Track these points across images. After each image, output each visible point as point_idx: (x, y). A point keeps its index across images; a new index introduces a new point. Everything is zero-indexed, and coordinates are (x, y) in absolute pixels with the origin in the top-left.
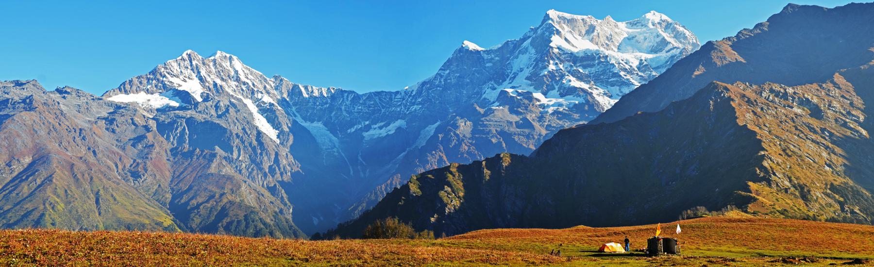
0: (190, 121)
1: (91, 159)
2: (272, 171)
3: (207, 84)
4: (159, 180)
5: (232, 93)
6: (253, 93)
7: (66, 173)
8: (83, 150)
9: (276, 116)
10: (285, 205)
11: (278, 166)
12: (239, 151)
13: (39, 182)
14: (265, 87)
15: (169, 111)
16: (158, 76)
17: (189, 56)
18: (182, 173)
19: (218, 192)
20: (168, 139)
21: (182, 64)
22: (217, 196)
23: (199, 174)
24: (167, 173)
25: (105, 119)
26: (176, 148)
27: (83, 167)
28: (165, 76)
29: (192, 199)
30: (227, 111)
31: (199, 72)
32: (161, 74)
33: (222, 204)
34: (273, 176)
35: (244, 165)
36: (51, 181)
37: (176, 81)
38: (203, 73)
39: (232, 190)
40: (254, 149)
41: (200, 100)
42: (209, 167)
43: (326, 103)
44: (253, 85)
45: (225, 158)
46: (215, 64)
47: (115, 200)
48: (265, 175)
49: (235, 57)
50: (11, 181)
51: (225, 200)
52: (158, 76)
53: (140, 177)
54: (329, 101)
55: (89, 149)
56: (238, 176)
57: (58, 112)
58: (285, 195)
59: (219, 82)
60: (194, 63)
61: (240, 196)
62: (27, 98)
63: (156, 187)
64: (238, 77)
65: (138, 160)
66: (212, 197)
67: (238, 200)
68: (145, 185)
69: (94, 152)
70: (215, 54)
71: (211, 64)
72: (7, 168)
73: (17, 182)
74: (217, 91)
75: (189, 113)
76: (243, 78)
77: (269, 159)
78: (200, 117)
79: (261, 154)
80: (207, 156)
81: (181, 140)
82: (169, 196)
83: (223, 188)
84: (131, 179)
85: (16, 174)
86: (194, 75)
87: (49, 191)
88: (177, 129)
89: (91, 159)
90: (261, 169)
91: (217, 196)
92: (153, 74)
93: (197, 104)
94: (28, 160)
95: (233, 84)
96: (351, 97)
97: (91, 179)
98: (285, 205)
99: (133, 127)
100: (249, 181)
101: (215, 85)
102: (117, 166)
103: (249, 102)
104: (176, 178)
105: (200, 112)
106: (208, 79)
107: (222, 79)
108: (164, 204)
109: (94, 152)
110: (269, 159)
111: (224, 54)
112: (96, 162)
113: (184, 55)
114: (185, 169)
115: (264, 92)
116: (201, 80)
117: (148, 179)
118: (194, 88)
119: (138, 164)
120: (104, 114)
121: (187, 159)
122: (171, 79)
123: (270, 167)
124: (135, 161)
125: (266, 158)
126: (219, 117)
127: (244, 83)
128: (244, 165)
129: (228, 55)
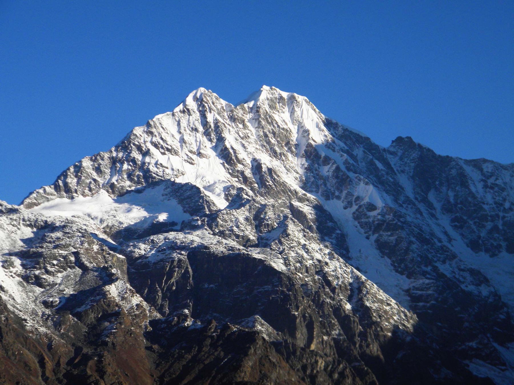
3: (240, 167)
12: (310, 327)
16: (136, 155)
17: (200, 101)
20: (150, 299)
21: (184, 123)
28: (146, 153)
31: (221, 139)
32: (139, 148)
35: (321, 364)
37: (176, 162)
38: (231, 140)
41: (220, 203)
45: (276, 345)
46: (257, 120)
49: (300, 98)
52: (136, 155)
59: (267, 161)
60: (210, 118)
65: (85, 350)
70: (255, 94)
74: (262, 182)
75: (196, 238)
79: (363, 335)
88: (170, 275)
99: (78, 271)
101: (257, 166)
102: (42, 363)
105: (222, 234)
106: (242, 155)
107: (274, 154)
113: (190, 101)
116: (227, 156)
119: (86, 358)
121: (189, 350)
122: (163, 159)
128: (321, 364)
129: (285, 95)
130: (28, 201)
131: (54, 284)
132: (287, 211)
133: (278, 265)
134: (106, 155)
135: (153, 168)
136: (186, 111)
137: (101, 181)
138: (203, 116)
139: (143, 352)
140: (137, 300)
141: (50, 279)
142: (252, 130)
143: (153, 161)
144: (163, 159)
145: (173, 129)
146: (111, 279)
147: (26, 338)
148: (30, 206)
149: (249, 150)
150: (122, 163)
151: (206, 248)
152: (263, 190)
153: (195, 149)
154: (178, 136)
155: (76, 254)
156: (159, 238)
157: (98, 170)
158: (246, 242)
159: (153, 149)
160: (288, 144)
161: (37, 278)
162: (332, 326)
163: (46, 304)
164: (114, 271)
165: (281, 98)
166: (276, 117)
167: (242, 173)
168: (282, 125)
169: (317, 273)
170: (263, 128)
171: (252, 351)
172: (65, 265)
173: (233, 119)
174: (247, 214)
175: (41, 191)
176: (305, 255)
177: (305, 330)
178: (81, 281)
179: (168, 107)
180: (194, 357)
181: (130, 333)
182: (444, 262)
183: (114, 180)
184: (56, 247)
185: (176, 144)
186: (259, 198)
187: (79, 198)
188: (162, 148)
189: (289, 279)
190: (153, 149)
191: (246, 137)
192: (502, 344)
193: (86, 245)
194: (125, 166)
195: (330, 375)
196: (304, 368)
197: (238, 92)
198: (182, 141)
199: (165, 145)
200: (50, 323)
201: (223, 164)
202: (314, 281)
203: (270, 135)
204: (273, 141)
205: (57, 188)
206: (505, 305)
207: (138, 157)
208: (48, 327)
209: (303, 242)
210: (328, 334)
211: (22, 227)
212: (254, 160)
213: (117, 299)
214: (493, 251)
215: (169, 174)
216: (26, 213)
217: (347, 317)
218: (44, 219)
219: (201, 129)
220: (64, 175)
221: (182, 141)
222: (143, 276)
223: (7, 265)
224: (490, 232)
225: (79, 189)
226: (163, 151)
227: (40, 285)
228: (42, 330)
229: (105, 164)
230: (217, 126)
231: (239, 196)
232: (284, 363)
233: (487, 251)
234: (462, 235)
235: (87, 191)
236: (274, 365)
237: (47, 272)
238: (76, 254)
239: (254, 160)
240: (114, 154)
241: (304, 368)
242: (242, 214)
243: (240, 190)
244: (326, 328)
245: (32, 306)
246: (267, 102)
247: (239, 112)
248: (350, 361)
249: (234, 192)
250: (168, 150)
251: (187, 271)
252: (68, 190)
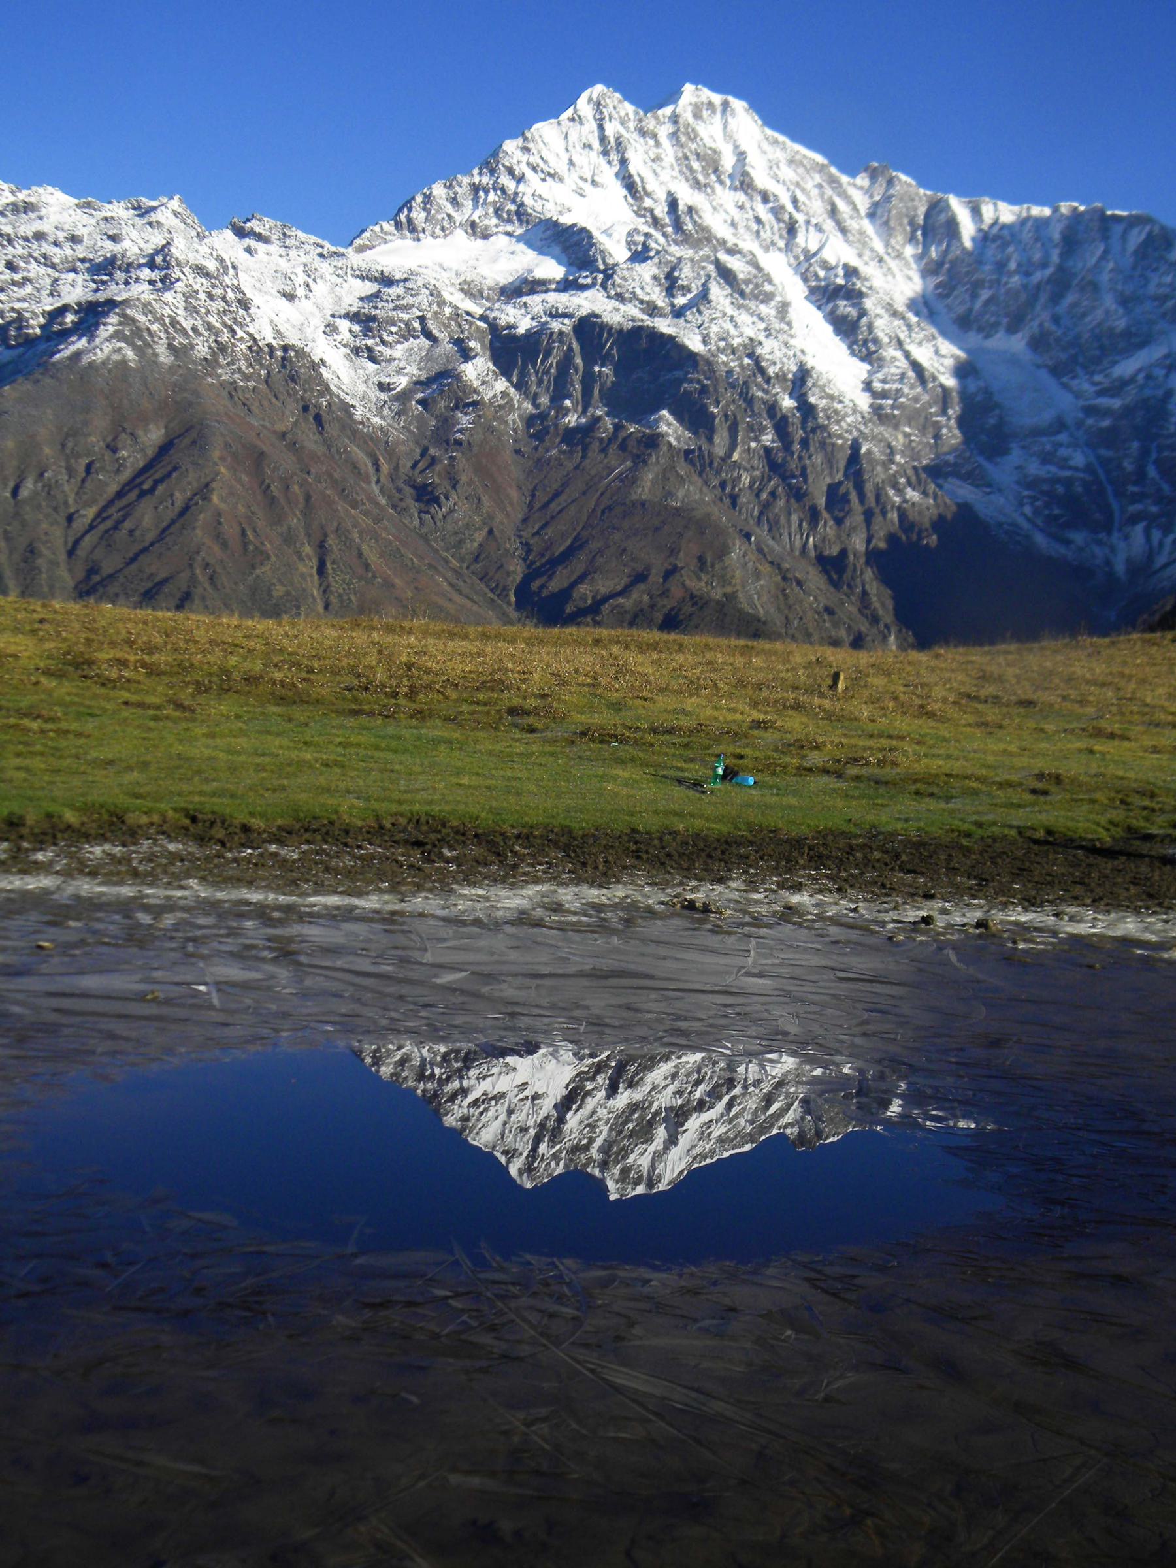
0: (588, 329)
1: (310, 439)
2: (835, 498)
3: (648, 202)
4: (491, 517)
5: (721, 230)
6: (792, 230)
7: (245, 478)
8: (291, 416)
9: (863, 313)
10: (875, 620)
11: (859, 487)
12: (733, 430)
13: (179, 498)
14: (833, 212)
15: (532, 292)
16: (505, 180)
17: (598, 105)
18: (557, 495)
19: (658, 565)
20: (520, 386)
21: (573, 137)
22: (656, 578)
23: (605, 502)
24: (514, 494)
25: (354, 317)
26: (543, 416)
27: (287, 462)
28: (520, 179)
29: (581, 578)
30: (704, 296)
31: (623, 162)
32: (510, 171)
33: (668, 604)
34: (839, 522)
35: (746, 479)
36: (206, 498)
39: (701, 559)
40: (781, 425)
41: (619, 253)
42: (634, 481)
43: (1044, 265)
44: (795, 201)
45: (688, 452)
46: (674, 135)
47: (367, 566)
48: (814, 516)
49: (739, 105)
50: (120, 494)
51: (677, 592)
52: (505, 180)
53: (436, 500)
54: (1055, 257)
55: (306, 409)
56: (722, 516)
57: (230, 295)
58: (873, 588)
59: (686, 196)
60: (611, 129)
61: (725, 581)
62: (157, 252)
63: (480, 536)
64: (745, 174)
65: (432, 452)
66: (640, 578)
67: (717, 594)
68: (449, 527)
69: (318, 418)
70: (673, 96)
71: (664, 131)
72: (108, 455)
73: (132, 496)
74: (678, 225)
76: (762, 179)
77: (830, 461)
78: (616, 314)
79: (805, 443)
80: (631, 444)
81: (559, 392)
82: (517, 569)
83: (673, 552)
84: (414, 507)
85: (126, 475)
86: (609, 175)
87: (199, 534)
88: (548, 354)
89: (310, 439)
90: (798, 495)
91: (656, 578)
92: (492, 172)
93: (609, 273)
94: (154, 435)
95: (728, 198)
96: (1136, 237)
97: (308, 498)
98: (875, 620)
99: (424, 342)
100: (761, 533)
101: (673, 204)
103: (779, 268)
104: (541, 507)
105: (620, 297)
107: (697, 185)
108: (502, 593)
109: (318, 418)
110: (830, 461)
111: (706, 94)
112: (321, 450)
113: (583, 105)
114: (565, 485)
115: (829, 225)
116: (630, 185)
117: (458, 508)
118: (607, 218)
119: (433, 461)
120: (351, 303)
123: (832, 490)
124: (424, 452)
125: (818, 459)
126: (678, 313)
127: (765, 198)
128: (746, 479)
129: (717, 98)
130: (358, 242)
131: (391, 360)
132: (711, 268)
133: (694, 344)
134: (466, 180)
135: (528, 201)
136: (576, 119)
137: (458, 217)
138: (601, 127)
139: (508, 455)
140: (501, 385)
141: (387, 352)
142: (669, 151)
143: (529, 191)
144: (544, 189)
145: (557, 143)
146: (466, 355)
147: (355, 432)
148: (361, 249)
149: (664, 180)
150: (487, 192)
151: (597, 316)
152: (679, 237)
153: (588, 176)
154: (565, 157)
155: (422, 319)
156: (535, 301)
157: (454, 201)
158: (652, 309)
159: (529, 174)
160: (716, 171)
161: (369, 349)
162: (762, 430)
163: (382, 387)
164: (472, 344)
165: (710, 105)
166: (702, 130)
167: (651, 211)
168: (709, 143)
169: (750, 356)
170: (682, 146)
171: (654, 459)
172: (407, 333)
173: (643, 133)
174: (655, 271)
175: (377, 228)
176: (733, 331)
177: (726, 434)
178: (428, 357)
179: (553, 112)
180: (576, 468)
181: (492, 430)
182: (920, 344)
183: (475, 217)
184: (396, 308)
185: (560, 166)
186: (673, 249)
187: (427, 240)
188: (542, 171)
189: (709, 363)
190: (529, 174)
191: (657, 159)
192: (989, 458)
193: (435, 307)
194: (492, 197)
195: (757, 496)
196: (723, 485)
197: (652, 94)
198: (571, 163)
199: (546, 168)
200: (386, 412)
201: (625, 197)
202: (741, 366)
203: (692, 158)
204: (696, 165)
205: (398, 225)
206: (997, 406)
207: (511, 185)
208: (383, 418)
209: (730, 311)
210: (756, 439)
211: (350, 278)
212: (670, 194)
213: (476, 383)
214: (988, 330)
215: (550, 211)
216: (354, 259)
217: (784, 418)
218: (380, 269)
219: (596, 144)
220: (408, 204)
221: (571, 163)
222: (510, 351)
223: (331, 330)
224: (988, 302)
225: (429, 228)
226: (543, 176)
227: (373, 359)
228: (377, 421)
229: (462, 190)
230: (619, 144)
231: (646, 248)
232: (695, 478)
233: (980, 329)
234: (949, 308)
235: (438, 231)
236: (682, 480)
237: (383, 342)
238: (422, 319)
239: (670, 194)
240: (476, 179)
241: (723, 485)
242: (647, 271)
243: (647, 235)
244: (756, 431)
245: (362, 388)
246: (690, 109)
247: (650, 123)
248: (784, 478)
249: (641, 239)
250: (550, 175)
251: (570, 349)
252: (412, 227)
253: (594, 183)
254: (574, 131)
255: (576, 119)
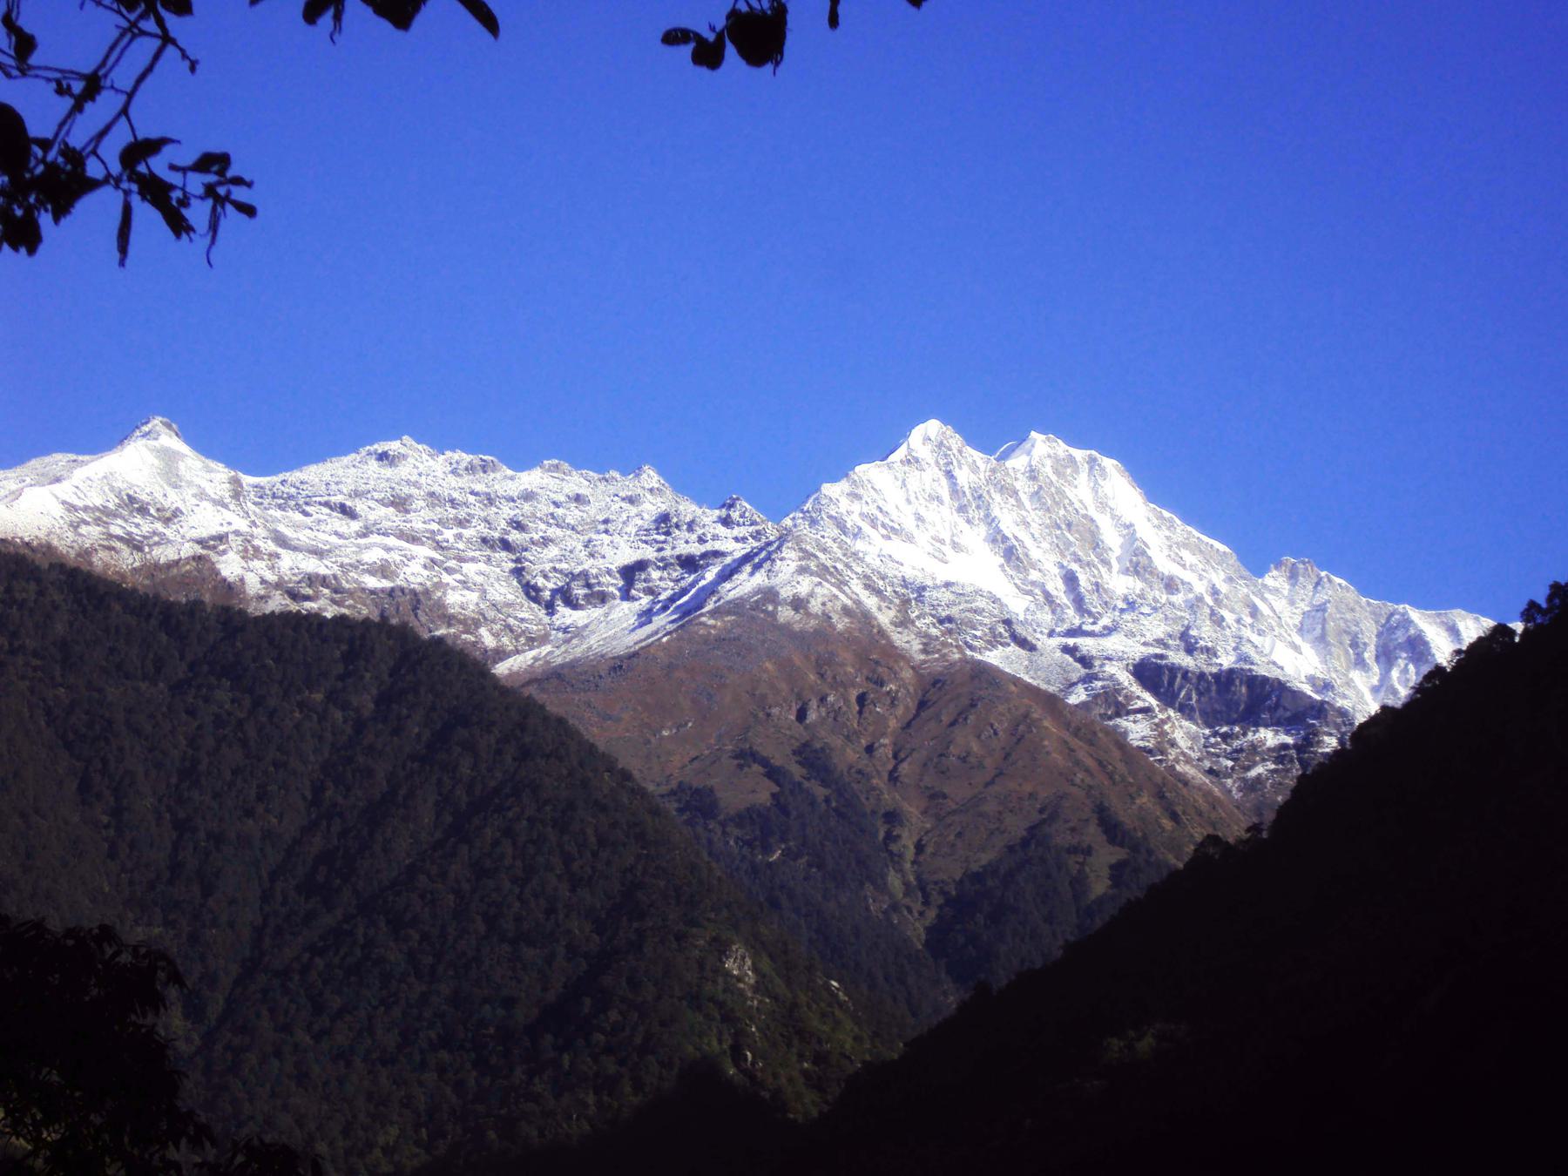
3: (1034, 575)
31: (990, 520)
49: (1109, 463)
71: (1023, 486)
86: (975, 537)
129: (1079, 454)
136: (911, 461)
159: (866, 528)
165: (1071, 459)
170: (1048, 510)
188: (884, 525)
199: (887, 521)
226: (884, 532)
246: (1048, 462)
253: (956, 546)
254: (914, 479)
255: (911, 461)
